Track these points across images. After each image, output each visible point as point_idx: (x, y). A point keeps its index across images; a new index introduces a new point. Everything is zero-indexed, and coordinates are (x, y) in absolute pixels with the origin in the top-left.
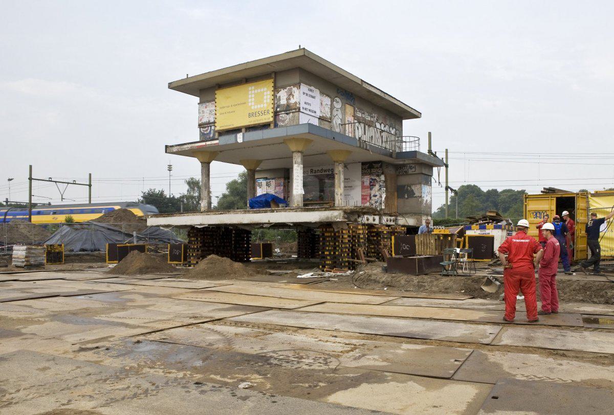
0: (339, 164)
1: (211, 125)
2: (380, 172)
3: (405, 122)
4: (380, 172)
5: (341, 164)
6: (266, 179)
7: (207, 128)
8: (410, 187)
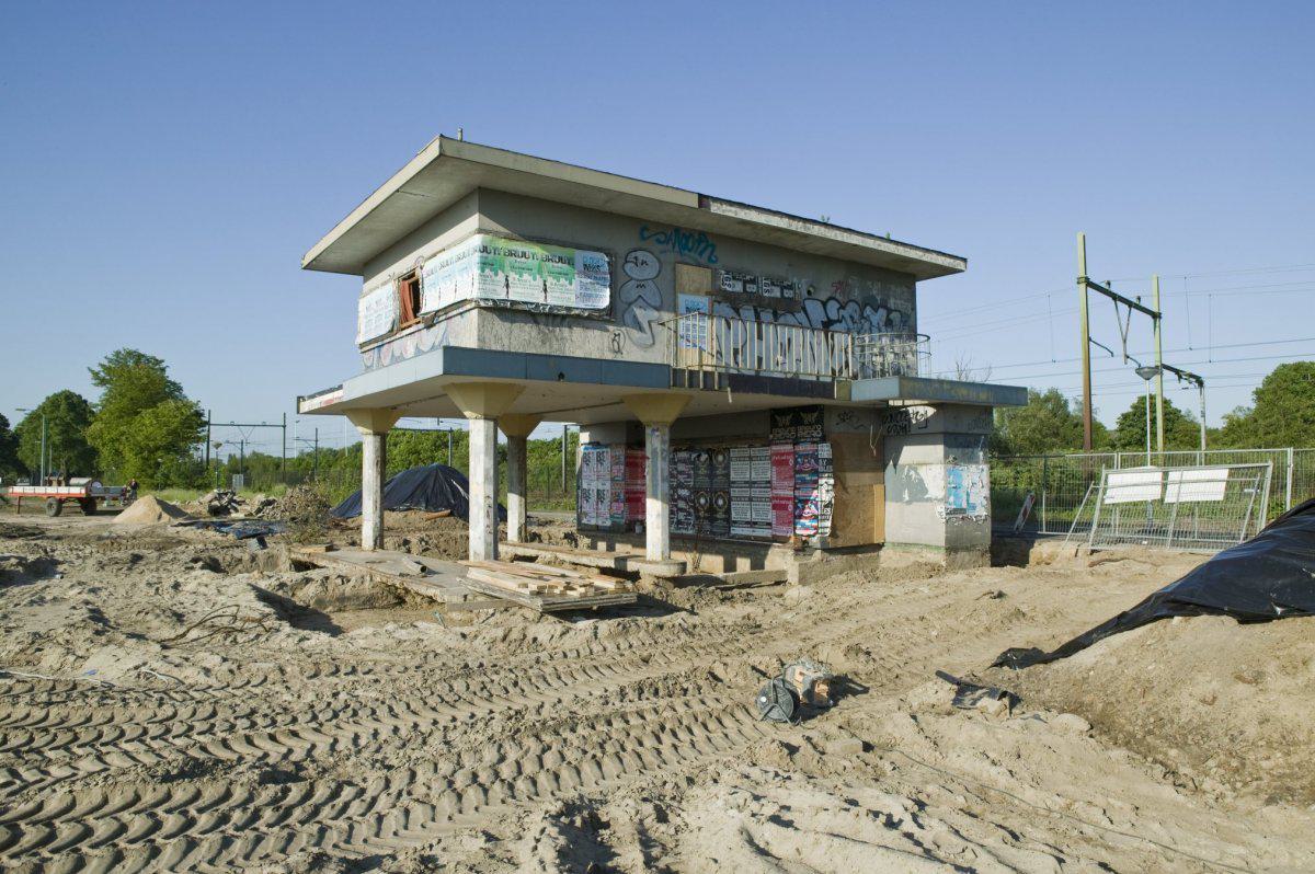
0: (654, 430)
2: (817, 434)
3: (918, 284)
4: (817, 434)
5: (657, 430)
8: (915, 470)
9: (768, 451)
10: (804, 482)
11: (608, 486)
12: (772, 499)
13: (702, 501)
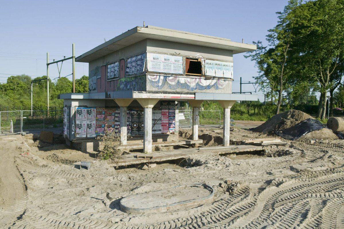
1: (161, 75)
6: (86, 107)
7: (155, 77)
9: (160, 111)
10: (171, 119)
11: (94, 122)
12: (161, 124)
13: (135, 125)
